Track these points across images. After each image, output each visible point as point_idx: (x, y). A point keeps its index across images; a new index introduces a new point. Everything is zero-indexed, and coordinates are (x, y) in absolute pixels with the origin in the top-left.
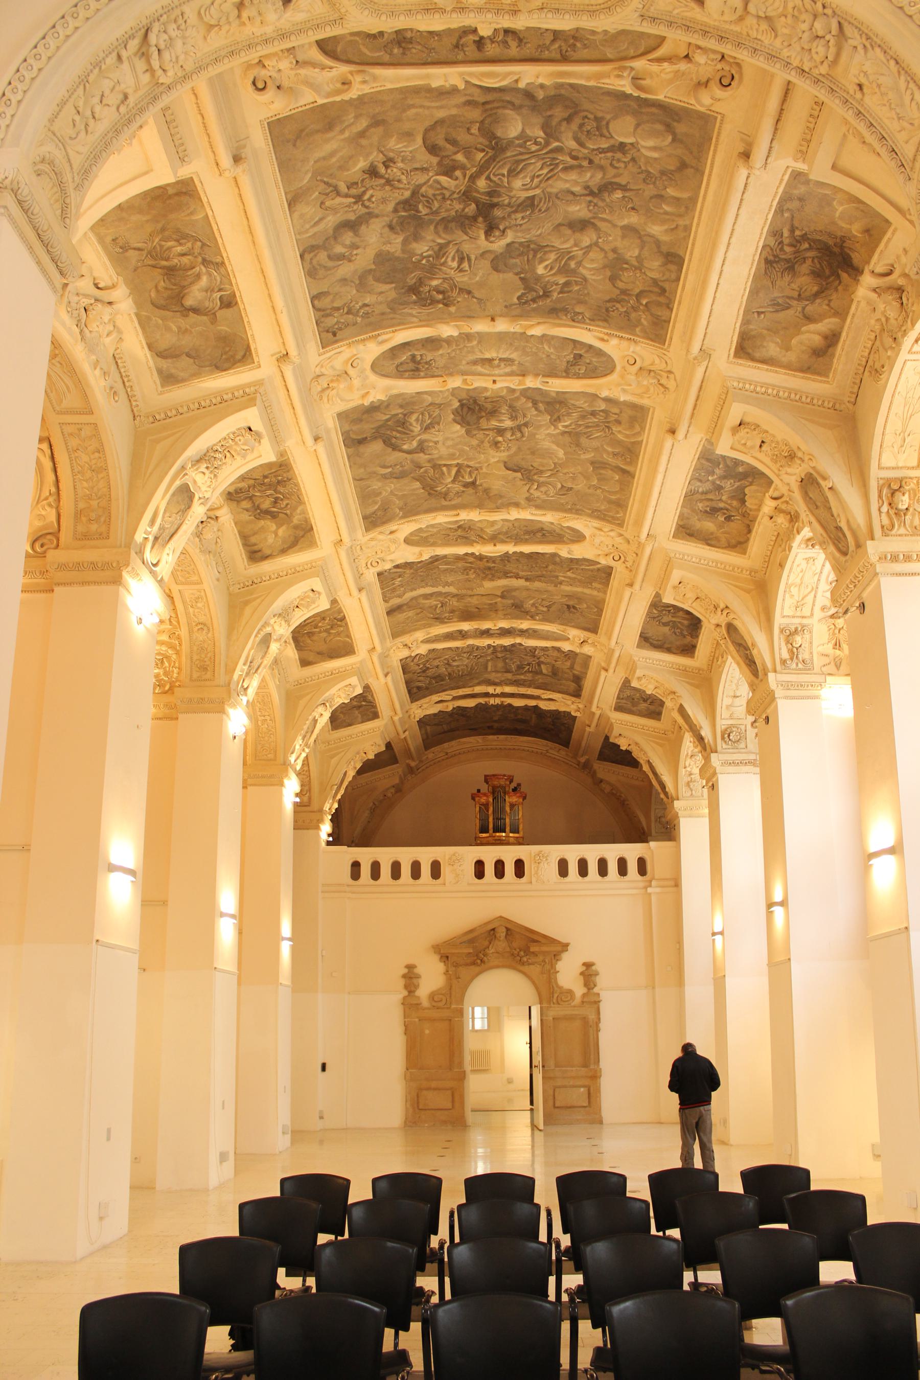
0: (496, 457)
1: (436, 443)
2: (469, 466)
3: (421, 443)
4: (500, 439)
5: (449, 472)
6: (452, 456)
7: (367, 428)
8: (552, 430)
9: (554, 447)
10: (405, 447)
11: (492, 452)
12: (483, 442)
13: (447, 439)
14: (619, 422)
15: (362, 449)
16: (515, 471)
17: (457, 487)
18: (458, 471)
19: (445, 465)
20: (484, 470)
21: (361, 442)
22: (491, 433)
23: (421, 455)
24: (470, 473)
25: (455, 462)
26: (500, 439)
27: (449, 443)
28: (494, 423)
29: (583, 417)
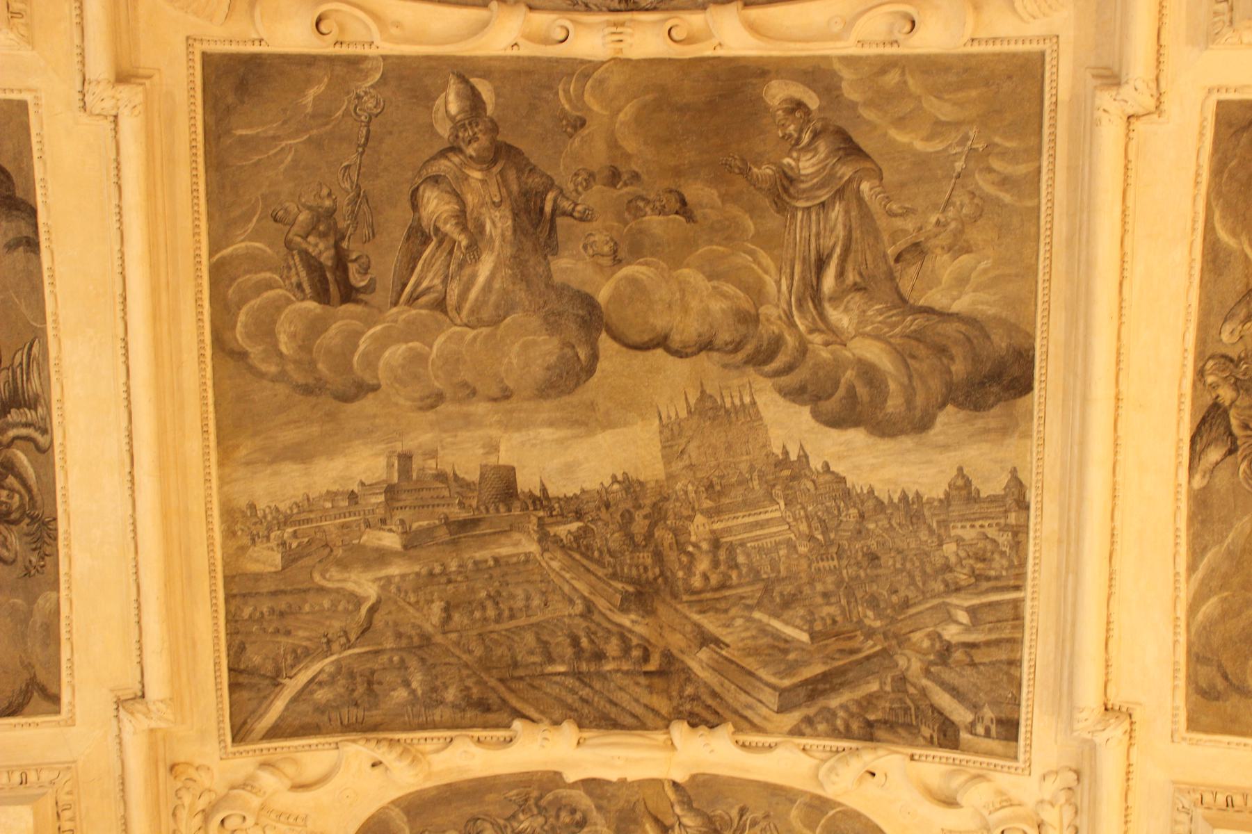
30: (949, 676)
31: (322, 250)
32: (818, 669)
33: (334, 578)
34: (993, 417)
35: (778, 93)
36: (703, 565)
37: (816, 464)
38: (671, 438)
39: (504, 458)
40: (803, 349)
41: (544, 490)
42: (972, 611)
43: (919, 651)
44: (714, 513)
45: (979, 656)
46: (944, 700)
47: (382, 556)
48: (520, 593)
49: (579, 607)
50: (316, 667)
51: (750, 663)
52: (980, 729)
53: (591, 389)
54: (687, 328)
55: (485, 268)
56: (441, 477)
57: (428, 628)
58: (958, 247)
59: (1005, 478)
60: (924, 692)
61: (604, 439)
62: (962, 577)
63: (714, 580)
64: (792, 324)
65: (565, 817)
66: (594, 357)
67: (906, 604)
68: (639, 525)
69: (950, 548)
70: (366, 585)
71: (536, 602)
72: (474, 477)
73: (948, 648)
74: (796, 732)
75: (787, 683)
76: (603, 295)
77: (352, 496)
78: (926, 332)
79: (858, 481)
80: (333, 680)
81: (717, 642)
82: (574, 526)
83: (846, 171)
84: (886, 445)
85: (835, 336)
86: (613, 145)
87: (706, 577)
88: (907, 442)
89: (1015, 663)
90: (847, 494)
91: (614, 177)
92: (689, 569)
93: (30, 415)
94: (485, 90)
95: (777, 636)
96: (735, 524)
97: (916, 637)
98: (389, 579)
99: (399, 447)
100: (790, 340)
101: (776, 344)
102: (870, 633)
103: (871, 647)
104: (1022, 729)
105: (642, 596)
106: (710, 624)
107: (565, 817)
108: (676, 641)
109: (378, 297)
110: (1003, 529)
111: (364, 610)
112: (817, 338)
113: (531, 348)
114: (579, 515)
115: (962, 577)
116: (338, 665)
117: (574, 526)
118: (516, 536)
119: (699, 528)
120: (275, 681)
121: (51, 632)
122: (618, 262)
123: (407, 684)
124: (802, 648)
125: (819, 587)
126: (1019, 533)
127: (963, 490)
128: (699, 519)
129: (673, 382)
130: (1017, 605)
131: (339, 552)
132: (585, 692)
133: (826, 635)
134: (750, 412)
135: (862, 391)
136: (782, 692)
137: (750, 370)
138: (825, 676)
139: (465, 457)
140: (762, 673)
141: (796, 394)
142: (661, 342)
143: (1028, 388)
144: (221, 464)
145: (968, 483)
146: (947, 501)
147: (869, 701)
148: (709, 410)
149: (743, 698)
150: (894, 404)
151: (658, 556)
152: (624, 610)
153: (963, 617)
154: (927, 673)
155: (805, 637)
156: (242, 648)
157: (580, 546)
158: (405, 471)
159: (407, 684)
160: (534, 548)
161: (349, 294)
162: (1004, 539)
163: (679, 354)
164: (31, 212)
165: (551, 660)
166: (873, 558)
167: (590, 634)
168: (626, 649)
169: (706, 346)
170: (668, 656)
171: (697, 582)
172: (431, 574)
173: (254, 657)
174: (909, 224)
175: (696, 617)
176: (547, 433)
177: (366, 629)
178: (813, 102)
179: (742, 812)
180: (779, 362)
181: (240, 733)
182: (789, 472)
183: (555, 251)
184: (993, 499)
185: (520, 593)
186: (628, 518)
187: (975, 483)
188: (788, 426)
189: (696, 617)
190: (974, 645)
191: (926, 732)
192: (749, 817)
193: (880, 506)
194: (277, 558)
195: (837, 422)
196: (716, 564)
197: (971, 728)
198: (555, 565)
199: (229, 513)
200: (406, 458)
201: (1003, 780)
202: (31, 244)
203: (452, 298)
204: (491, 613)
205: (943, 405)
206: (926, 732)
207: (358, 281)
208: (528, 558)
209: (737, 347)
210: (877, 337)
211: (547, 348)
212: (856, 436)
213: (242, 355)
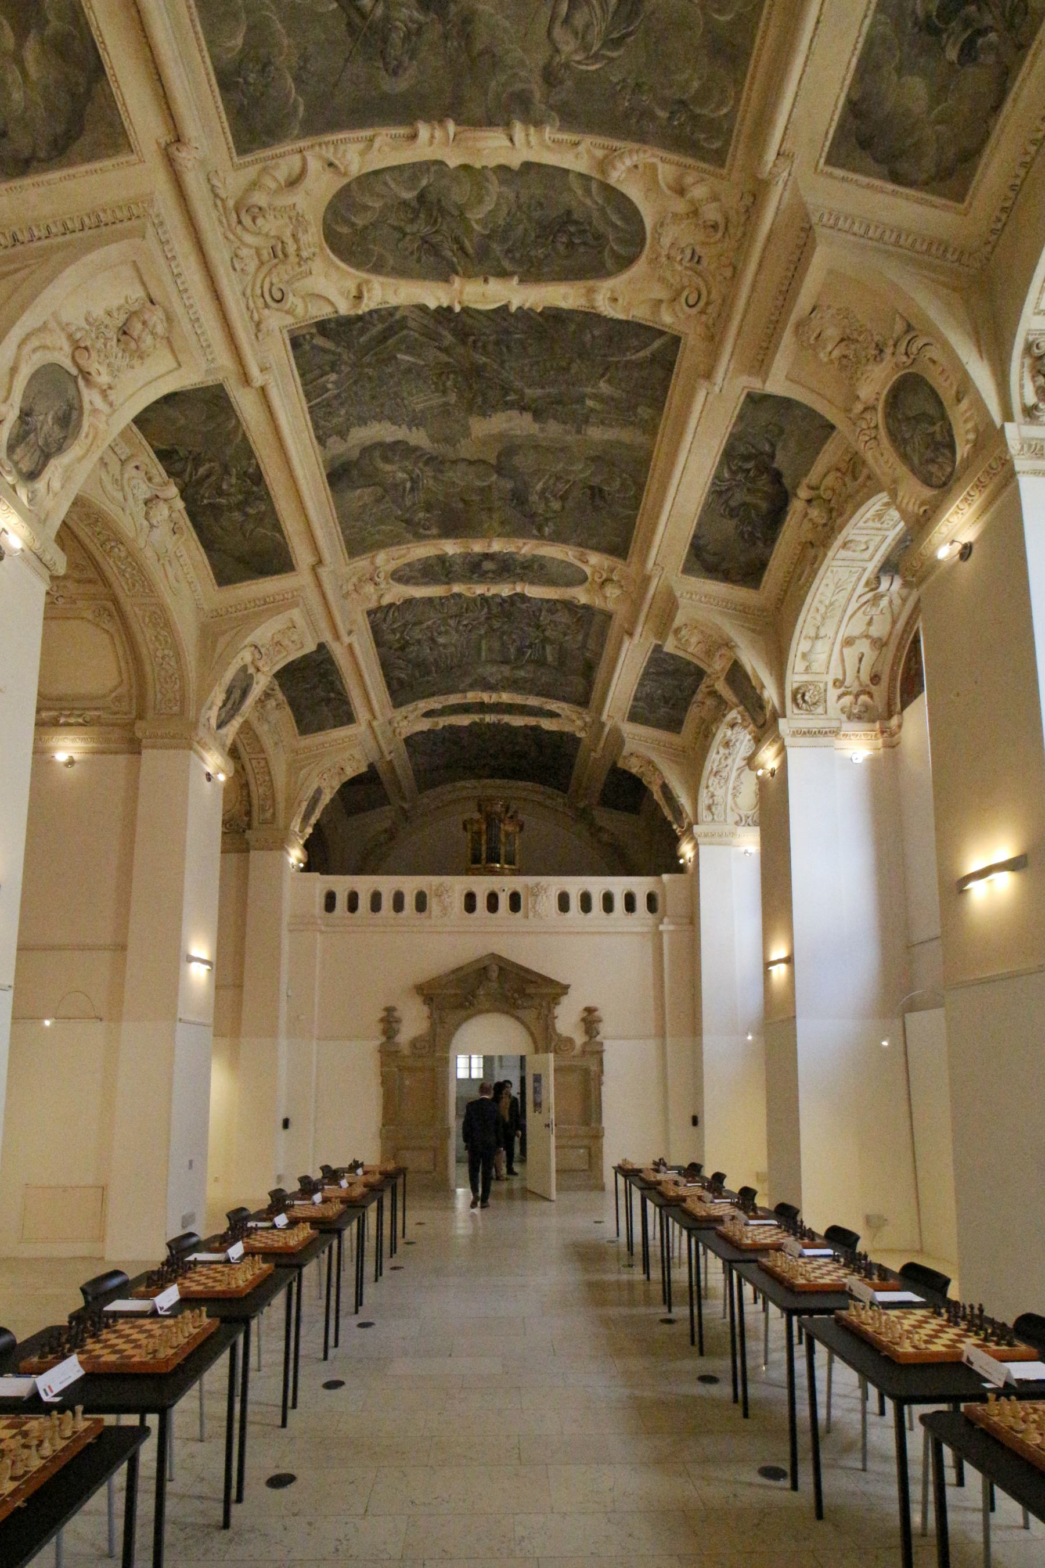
30: (329, 357)
31: (598, 502)
32: (390, 342)
33: (617, 394)
34: (337, 463)
35: (434, 531)
36: (449, 383)
37: (404, 426)
38: (466, 432)
39: (537, 426)
40: (415, 463)
41: (521, 413)
42: (327, 390)
43: (346, 363)
44: (446, 404)
45: (317, 372)
46: (329, 345)
47: (595, 397)
48: (534, 373)
49: (507, 365)
50: (633, 357)
51: (422, 339)
52: (308, 337)
54: (463, 466)
55: (539, 487)
56: (565, 423)
57: (578, 361)
58: (365, 505)
59: (328, 444)
60: (338, 345)
61: (495, 431)
62: (335, 403)
63: (444, 377)
64: (420, 470)
65: (518, 255)
66: (498, 457)
67: (355, 383)
68: (479, 400)
69: (343, 412)
70: (604, 387)
71: (526, 369)
72: (551, 421)
73: (333, 370)
74: (396, 308)
75: (405, 332)
76: (495, 476)
77: (603, 423)
78: (370, 478)
79: (387, 424)
80: (628, 349)
81: (439, 349)
82: (508, 398)
83: (407, 515)
85: (404, 470)
86: (491, 518)
87: (448, 378)
88: (368, 443)
89: (302, 376)
90: (390, 419)
91: (490, 509)
92: (455, 382)
93: (718, 488)
94: (535, 532)
95: (411, 354)
96: (437, 400)
97: (348, 369)
98: (593, 387)
99: (580, 437)
100: (420, 465)
102: (369, 365)
103: (367, 359)
104: (289, 347)
105: (477, 371)
106: (444, 358)
107: (518, 255)
108: (460, 350)
109: (581, 485)
110: (324, 427)
111: (606, 378)
112: (410, 468)
113: (523, 462)
114: (506, 403)
115: (335, 403)
116: (625, 355)
117: (508, 398)
118: (535, 396)
119: (453, 398)
120: (653, 359)
121: (741, 417)
122: (489, 486)
123: (593, 337)
124: (400, 350)
125: (396, 379)
126: (316, 427)
127: (343, 434)
128: (453, 402)
129: (466, 449)
130: (309, 400)
131: (613, 404)
132: (505, 324)
133: (389, 359)
134: (433, 439)
135: (390, 454)
136: (406, 327)
137: (435, 454)
138: (385, 339)
139: (554, 428)
140: (417, 335)
141: (416, 449)
142: (471, 463)
143: (329, 476)
144: (652, 452)
147: (362, 331)
148: (449, 440)
149: (425, 322)
150: (377, 453)
151: (470, 387)
152: (485, 364)
153: (330, 386)
154: (340, 355)
155: (399, 356)
156: (664, 379)
157: (506, 390)
159: (593, 337)
160: (527, 391)
161: (591, 488)
163: (464, 460)
164: (692, 545)
165: (521, 342)
166: (373, 397)
167: (501, 353)
168: (484, 347)
169: (454, 462)
170: (464, 343)
171: (452, 376)
172: (573, 385)
173: (660, 374)
174: (382, 507)
175: (451, 360)
176: (519, 432)
177: (607, 369)
178: (421, 530)
179: (419, 261)
181: (676, 340)
182: (416, 421)
183: (512, 490)
184: (330, 436)
185: (534, 373)
186: (484, 401)
187: (338, 439)
188: (418, 438)
189: (451, 360)
190: (322, 376)
191: (333, 325)
192: (415, 257)
193: (374, 418)
194: (639, 410)
195: (397, 443)
196: (444, 385)
197: (312, 336)
198: (517, 383)
199: (654, 433)
200: (579, 432)
201: (289, 320)
202: (695, 537)
203: (553, 478)
204: (548, 364)
205: (358, 459)
206: (333, 325)
207: (589, 492)
208: (529, 387)
209: (442, 463)
210: (387, 473)
211: (517, 460)
212: (389, 439)
213: (635, 483)
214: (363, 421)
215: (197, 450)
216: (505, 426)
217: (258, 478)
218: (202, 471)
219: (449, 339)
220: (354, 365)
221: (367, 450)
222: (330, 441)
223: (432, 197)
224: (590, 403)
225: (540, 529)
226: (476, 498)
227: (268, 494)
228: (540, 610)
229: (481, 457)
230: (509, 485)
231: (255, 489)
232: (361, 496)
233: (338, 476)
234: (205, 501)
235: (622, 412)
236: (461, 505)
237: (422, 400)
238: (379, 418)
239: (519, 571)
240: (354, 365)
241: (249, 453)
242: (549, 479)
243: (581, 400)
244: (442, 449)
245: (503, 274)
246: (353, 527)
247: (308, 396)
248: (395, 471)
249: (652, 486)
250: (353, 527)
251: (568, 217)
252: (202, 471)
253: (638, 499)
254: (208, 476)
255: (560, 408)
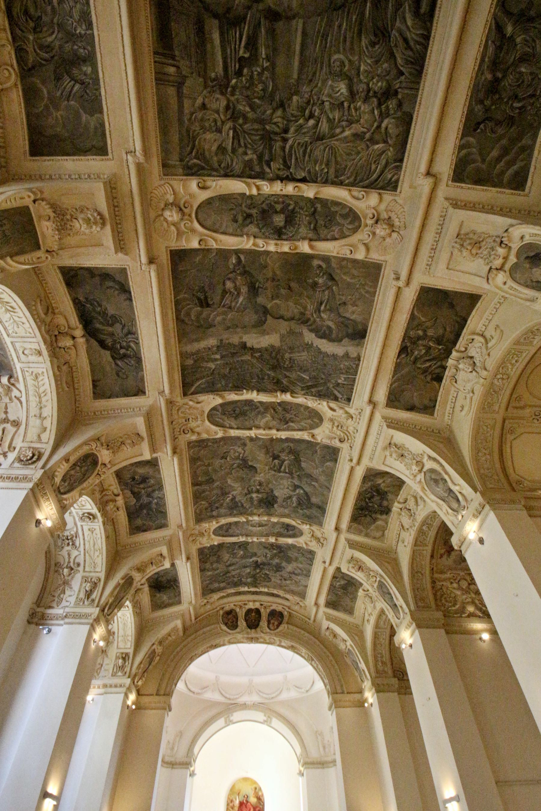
0: (259, 478)
1: (288, 488)
2: (275, 471)
3: (294, 490)
4: (258, 487)
5: (285, 469)
6: (282, 478)
7: (314, 511)
8: (234, 493)
9: (233, 485)
10: (302, 491)
11: (263, 480)
12: (267, 486)
13: (283, 489)
14: (206, 509)
15: (320, 504)
16: (252, 466)
17: (283, 456)
18: (281, 467)
19: (286, 473)
20: (267, 468)
21: (319, 507)
22: (263, 491)
23: (296, 483)
24: (274, 467)
25: (281, 474)
26: (258, 487)
27: (282, 487)
28: (260, 496)
29: (222, 505)
37: (315, 345)
38: (282, 337)
53: (265, 327)
56: (229, 344)
61: (267, 337)
79: (323, 350)
84: (330, 344)
88: (336, 344)
99: (220, 338)
101: (308, 320)
126: (358, 365)
127: (347, 355)
134: (301, 334)
135: (327, 332)
139: (235, 340)
141: (311, 331)
145: (348, 354)
146: (343, 356)
148: (291, 332)
158: (221, 343)
162: (354, 366)
180: (308, 324)
182: (309, 346)
188: (309, 337)
194: (192, 362)
195: (321, 337)
200: (221, 340)
212: (324, 341)
214: (335, 357)
215: (422, 377)
216: (261, 339)
217: (403, 350)
218: (428, 364)
219: (285, 381)
220: (329, 381)
221: (339, 340)
222: (355, 355)
223: (284, 423)
224: (218, 357)
225: (239, 261)
226: (283, 291)
227: (404, 340)
228: (234, 151)
229: (276, 321)
230: (260, 300)
231: (408, 344)
232: (353, 313)
233: (359, 334)
234: (440, 347)
235: (199, 358)
236: (293, 284)
237: (303, 357)
238: (326, 355)
239: (254, 212)
240: (329, 381)
241: (398, 367)
242: (235, 306)
243: (222, 357)
244: (297, 328)
245: (261, 403)
246: (367, 292)
247: (354, 380)
248: (328, 320)
249: (172, 325)
250: (367, 292)
251: (236, 418)
252: (428, 364)
253: (178, 311)
254: (427, 360)
255: (233, 351)
